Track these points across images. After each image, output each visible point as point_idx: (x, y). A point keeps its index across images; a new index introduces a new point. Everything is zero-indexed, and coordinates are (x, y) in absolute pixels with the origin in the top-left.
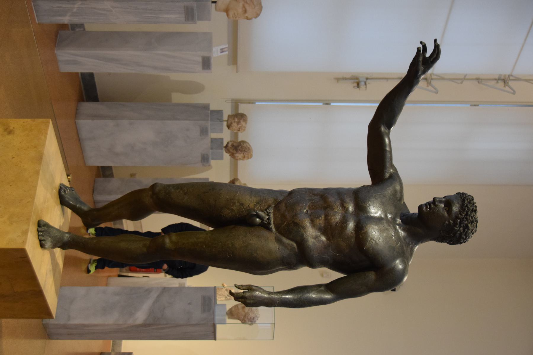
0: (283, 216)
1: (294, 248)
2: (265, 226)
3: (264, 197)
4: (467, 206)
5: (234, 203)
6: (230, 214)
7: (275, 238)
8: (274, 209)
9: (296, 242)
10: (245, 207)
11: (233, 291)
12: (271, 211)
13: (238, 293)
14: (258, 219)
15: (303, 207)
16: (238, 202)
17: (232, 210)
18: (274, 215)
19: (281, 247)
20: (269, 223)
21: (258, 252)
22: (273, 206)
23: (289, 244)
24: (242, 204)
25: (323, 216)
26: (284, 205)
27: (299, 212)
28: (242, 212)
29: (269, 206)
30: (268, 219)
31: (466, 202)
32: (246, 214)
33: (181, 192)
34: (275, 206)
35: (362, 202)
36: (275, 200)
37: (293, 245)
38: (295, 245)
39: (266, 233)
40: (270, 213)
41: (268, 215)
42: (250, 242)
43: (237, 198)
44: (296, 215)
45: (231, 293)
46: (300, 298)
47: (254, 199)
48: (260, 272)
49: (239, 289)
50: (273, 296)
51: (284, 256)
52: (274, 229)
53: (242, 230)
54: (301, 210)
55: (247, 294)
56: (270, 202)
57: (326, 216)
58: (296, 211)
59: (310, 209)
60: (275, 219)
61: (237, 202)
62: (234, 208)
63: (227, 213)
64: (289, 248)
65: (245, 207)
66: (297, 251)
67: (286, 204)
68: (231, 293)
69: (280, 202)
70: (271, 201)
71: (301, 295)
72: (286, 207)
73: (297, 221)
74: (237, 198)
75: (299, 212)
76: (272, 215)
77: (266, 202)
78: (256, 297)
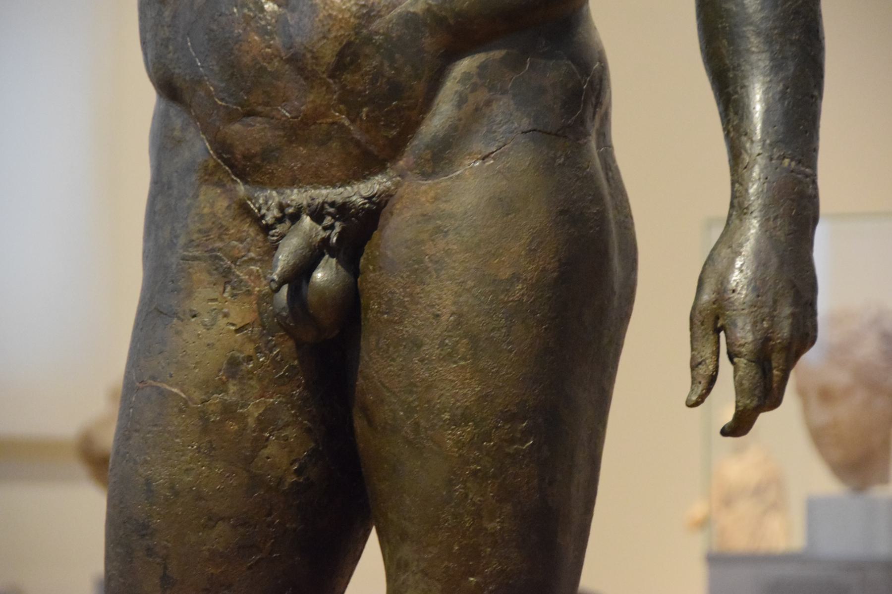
0: (298, 130)
1: (482, 67)
2: (356, 232)
3: (186, 246)
5: (228, 411)
6: (291, 433)
7: (425, 176)
8: (262, 186)
9: (452, 55)
10: (249, 349)
11: (728, 415)
12: (269, 201)
13: (740, 390)
14: (319, 275)
15: (248, 20)
16: (221, 387)
17: (266, 422)
18: (294, 182)
19: (478, 146)
20: (343, 210)
21: (505, 273)
22: (241, 189)
23: (462, 101)
24: (233, 365)
26: (237, 126)
27: (277, 41)
28: (276, 364)
29: (244, 210)
30: (318, 215)
32: (291, 343)
34: (243, 176)
36: (209, 176)
37: (467, 76)
38: (465, 65)
39: (396, 234)
40: (281, 207)
41: (295, 218)
42: (447, 318)
43: (198, 395)
44: (295, 60)
45: (739, 427)
46: (769, 40)
47: (205, 295)
48: (616, 263)
49: (712, 380)
50: (753, 189)
51: (526, 123)
52: (376, 185)
53: (380, 367)
54: (263, 32)
55: (745, 334)
56: (222, 204)
58: (270, 58)
60: (319, 179)
61: (217, 398)
62: (253, 411)
63: (283, 453)
64: (483, 95)
65: (249, 349)
66: (497, 54)
67: (231, 117)
68: (739, 427)
69: (223, 148)
70: (214, 202)
71: (749, 30)
72: (249, 114)
73: (329, 53)
74: (198, 395)
75: (277, 41)
76: (296, 196)
77: (223, 231)
78: (758, 285)
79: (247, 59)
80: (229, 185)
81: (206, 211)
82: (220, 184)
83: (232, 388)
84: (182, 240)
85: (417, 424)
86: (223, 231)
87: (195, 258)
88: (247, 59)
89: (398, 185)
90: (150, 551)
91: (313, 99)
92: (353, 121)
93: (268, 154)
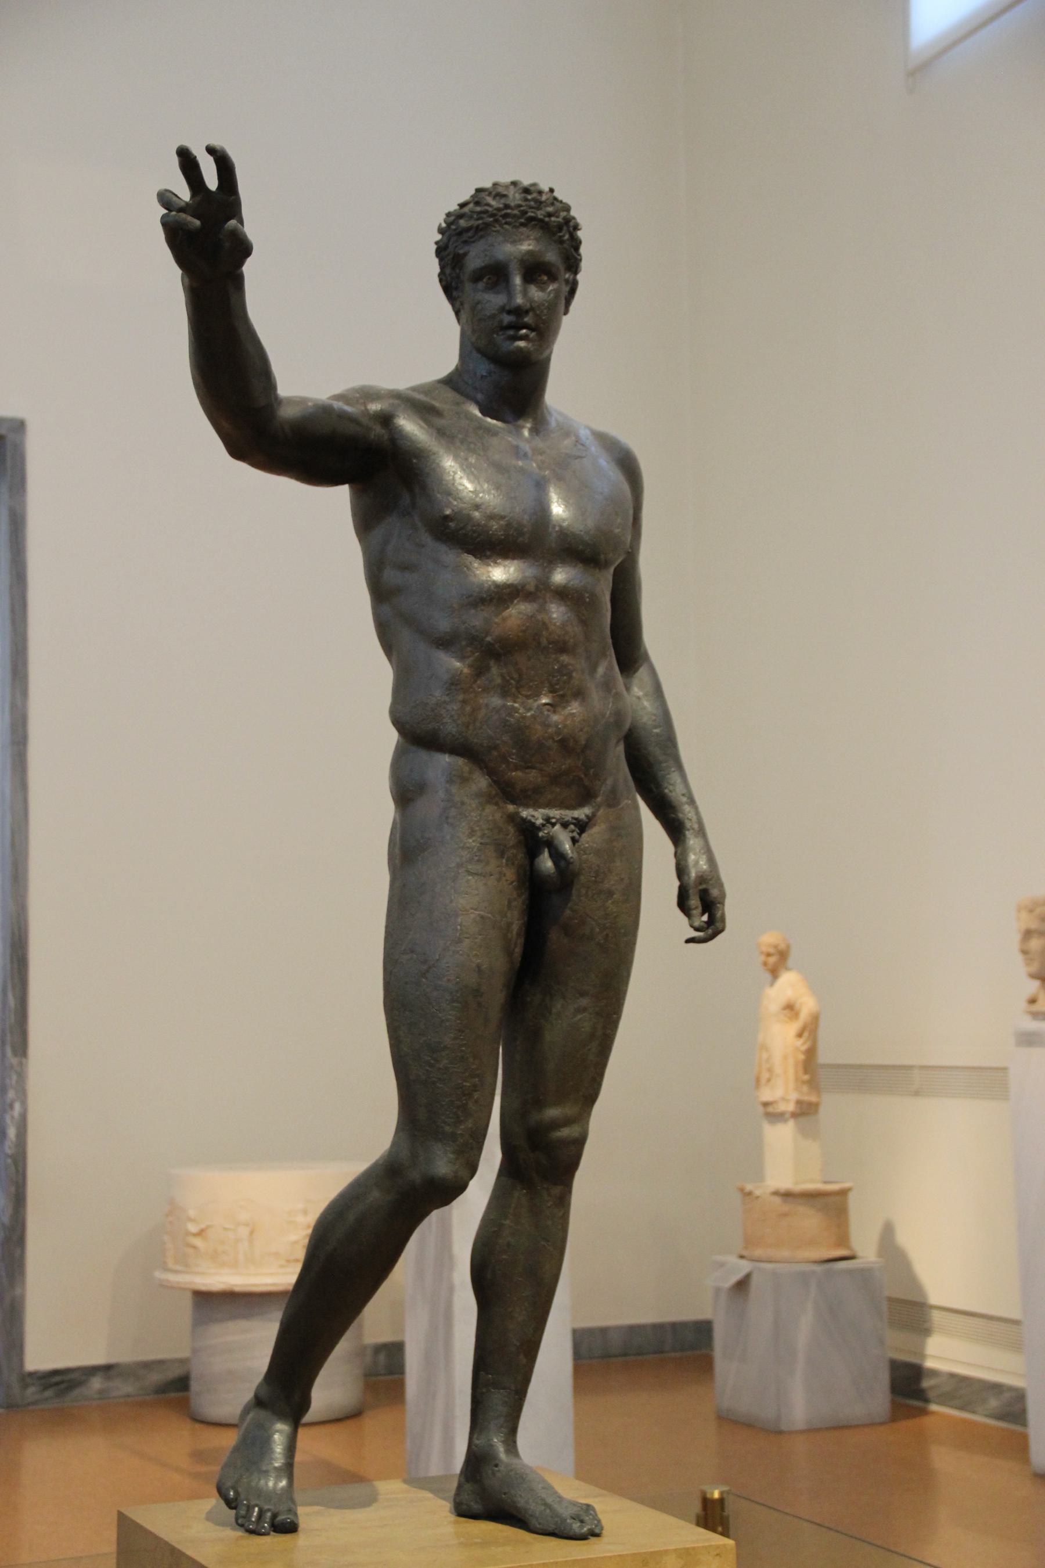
0: (555, 779)
4: (550, 215)
7: (610, 806)
17: (518, 935)
18: (549, 805)
22: (511, 808)
24: (510, 902)
25: (565, 658)
26: (520, 774)
30: (565, 825)
31: (540, 214)
33: (476, 1095)
35: (521, 534)
36: (490, 799)
41: (553, 825)
56: (498, 816)
57: (563, 648)
59: (537, 695)
67: (516, 769)
70: (493, 813)
76: (555, 813)
79: (534, 738)
80: (501, 804)
81: (490, 818)
82: (497, 804)
83: (509, 915)
84: (479, 834)
85: (607, 935)
86: (500, 830)
87: (487, 844)
88: (534, 738)
89: (598, 810)
90: (479, 1004)
91: (567, 763)
92: (586, 775)
93: (537, 790)
